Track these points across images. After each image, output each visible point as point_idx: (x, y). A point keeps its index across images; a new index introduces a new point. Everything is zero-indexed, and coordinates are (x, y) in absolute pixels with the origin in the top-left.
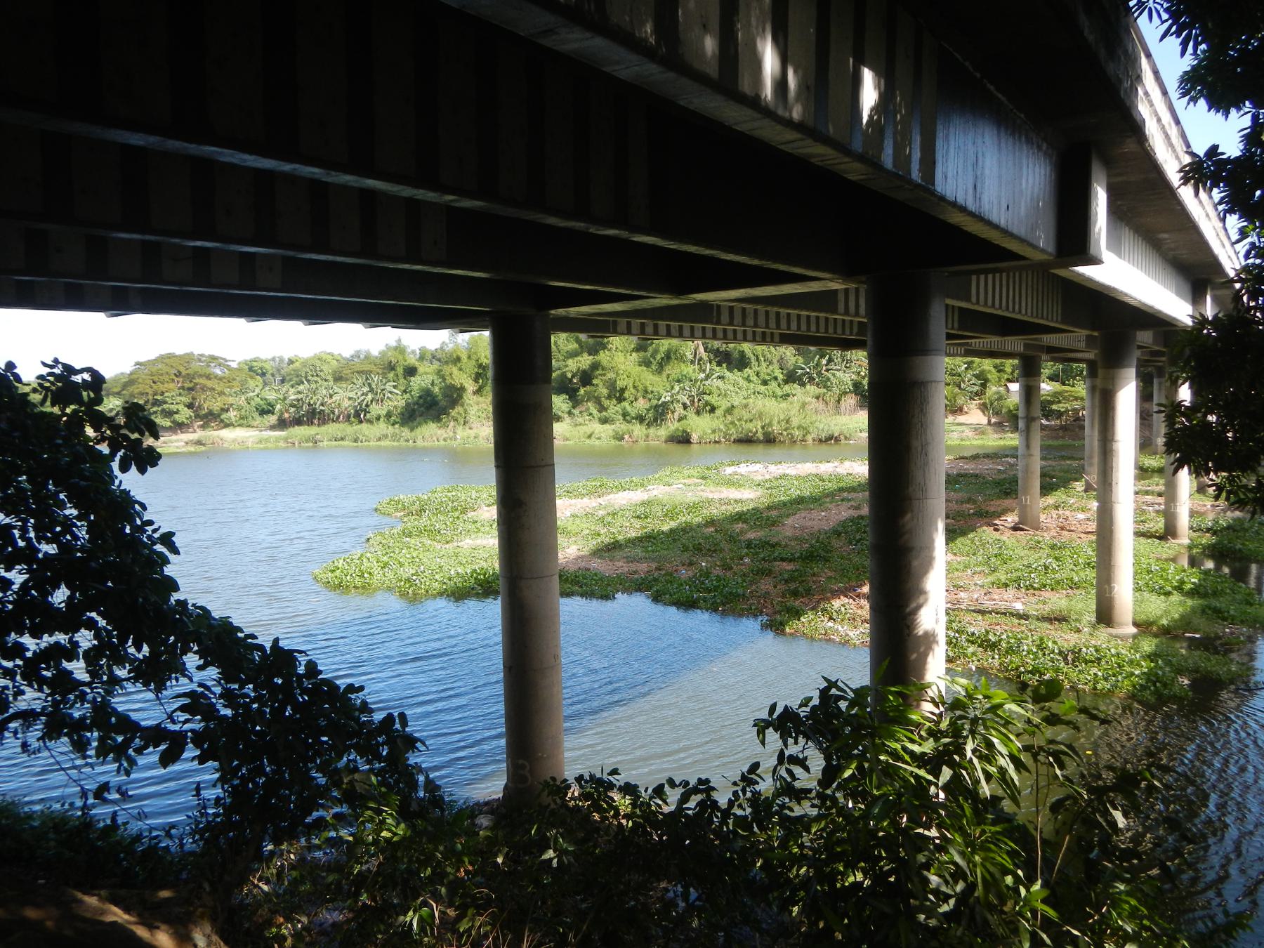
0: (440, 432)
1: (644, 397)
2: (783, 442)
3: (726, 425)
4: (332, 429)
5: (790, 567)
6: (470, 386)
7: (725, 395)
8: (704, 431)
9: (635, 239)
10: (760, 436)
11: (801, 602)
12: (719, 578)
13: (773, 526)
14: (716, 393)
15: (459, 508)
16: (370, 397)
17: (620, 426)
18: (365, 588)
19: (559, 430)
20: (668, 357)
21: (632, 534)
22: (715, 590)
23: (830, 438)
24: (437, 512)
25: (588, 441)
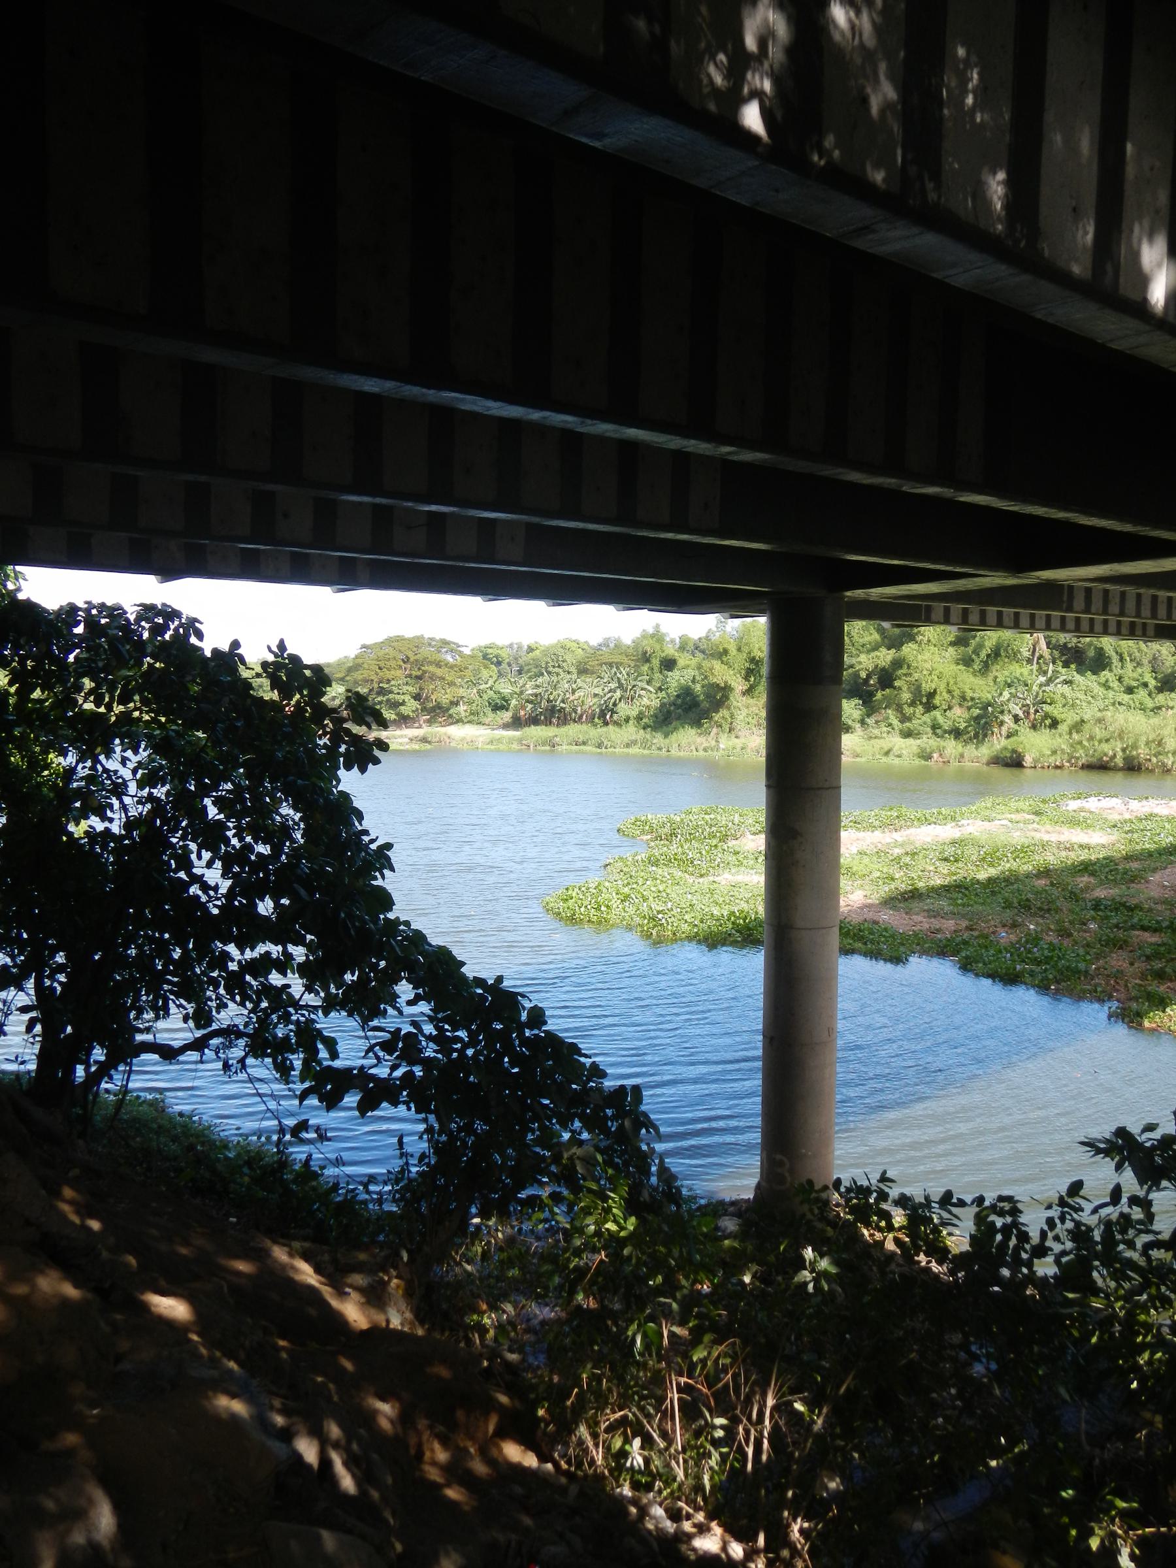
0: (699, 740)
1: (960, 705)
2: (1152, 771)
3: (1072, 746)
4: (572, 730)
5: (1154, 939)
6: (739, 685)
7: (1073, 705)
8: (1040, 752)
9: (962, 499)
10: (1119, 761)
11: (1169, 988)
12: (1051, 945)
13: (1133, 882)
14: (1062, 701)
15: (718, 834)
16: (618, 694)
17: (928, 741)
18: (601, 924)
19: (847, 743)
20: (996, 654)
21: (938, 881)
22: (1048, 960)
24: (691, 837)
25: (884, 759)
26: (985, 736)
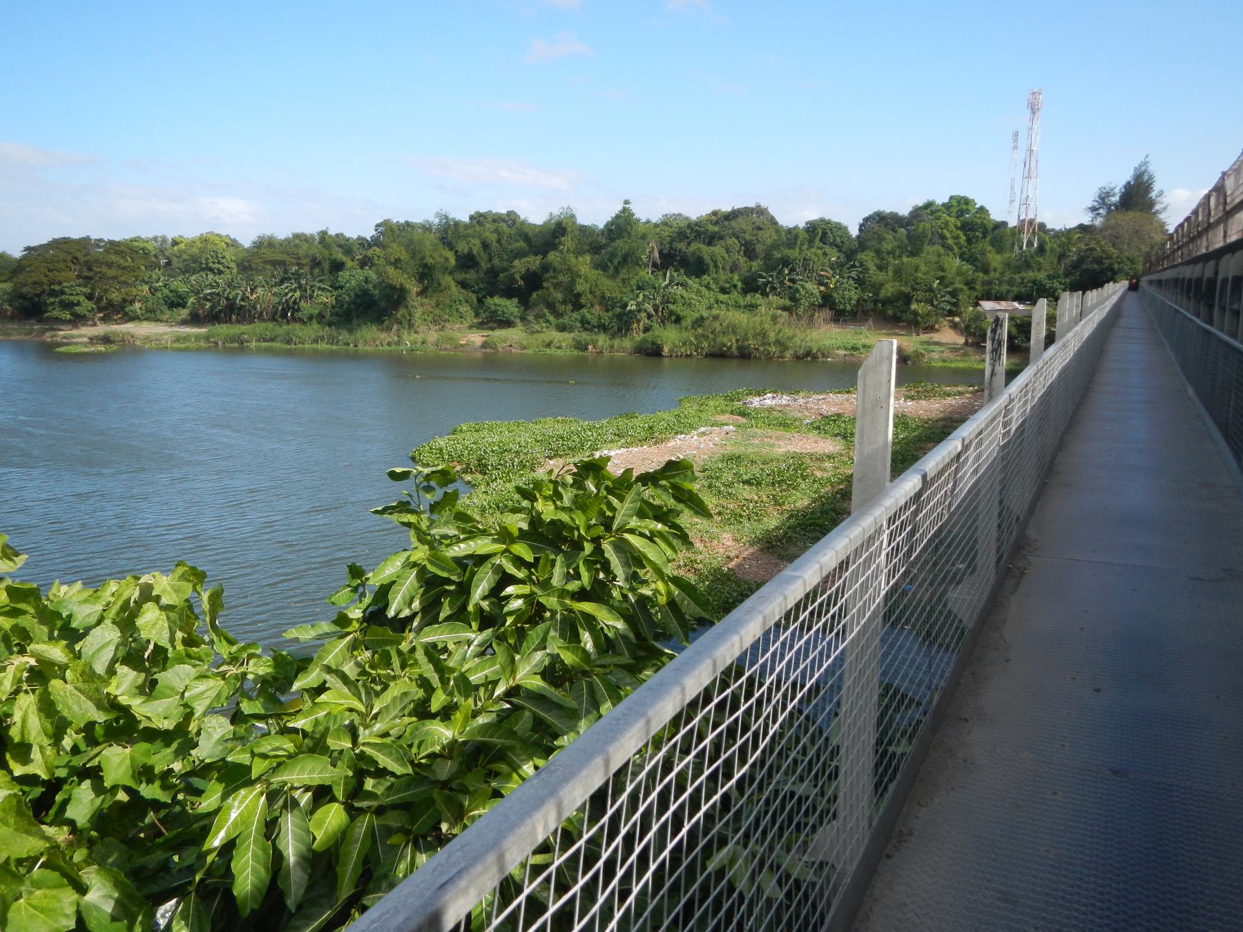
0: (383, 335)
4: (259, 327)
6: (413, 288)
8: (674, 344)
16: (298, 294)
20: (625, 260)
23: (808, 354)
26: (627, 330)
